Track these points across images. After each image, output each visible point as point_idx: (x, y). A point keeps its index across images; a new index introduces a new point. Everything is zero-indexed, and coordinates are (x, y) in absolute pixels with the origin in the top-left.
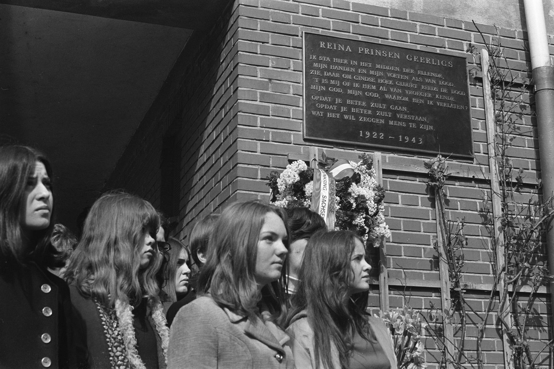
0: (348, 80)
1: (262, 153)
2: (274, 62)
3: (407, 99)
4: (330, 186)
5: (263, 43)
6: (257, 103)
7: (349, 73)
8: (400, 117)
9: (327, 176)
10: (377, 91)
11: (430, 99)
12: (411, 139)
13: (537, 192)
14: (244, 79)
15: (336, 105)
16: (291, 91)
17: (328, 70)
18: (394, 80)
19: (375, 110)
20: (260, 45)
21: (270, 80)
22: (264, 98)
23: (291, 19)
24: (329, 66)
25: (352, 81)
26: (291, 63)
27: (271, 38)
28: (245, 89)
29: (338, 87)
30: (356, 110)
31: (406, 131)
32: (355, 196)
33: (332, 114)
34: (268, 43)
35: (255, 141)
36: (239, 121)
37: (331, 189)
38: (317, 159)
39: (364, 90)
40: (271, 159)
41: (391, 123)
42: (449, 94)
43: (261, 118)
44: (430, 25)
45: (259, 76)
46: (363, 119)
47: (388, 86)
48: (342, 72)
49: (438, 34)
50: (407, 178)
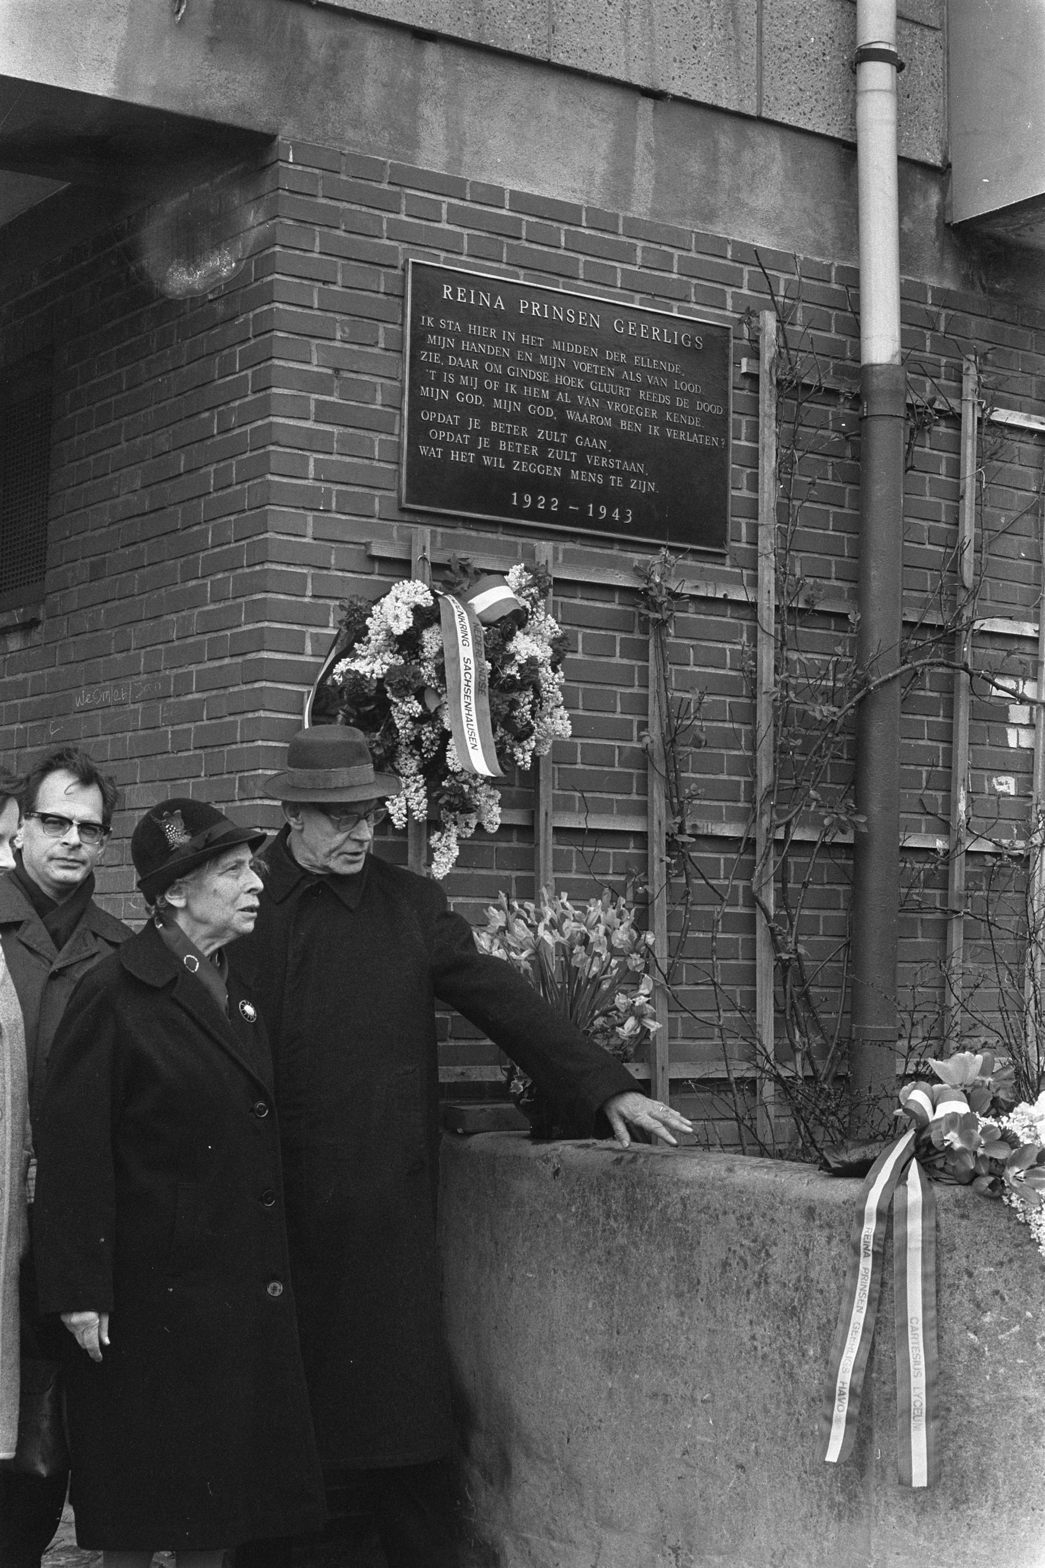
0: (494, 376)
1: (315, 539)
2: (347, 330)
3: (609, 422)
4: (474, 637)
5: (325, 282)
6: (309, 424)
7: (494, 359)
8: (593, 461)
9: (465, 615)
10: (552, 403)
11: (654, 422)
12: (610, 511)
13: (790, 1113)
14: (284, 367)
15: (468, 432)
16: (379, 398)
17: (458, 353)
18: (587, 377)
19: (544, 446)
20: (320, 288)
21: (337, 370)
22: (325, 412)
23: (385, 227)
24: (458, 343)
25: (504, 378)
26: (381, 332)
27: (341, 273)
28: (286, 392)
29: (474, 392)
30: (507, 446)
31: (603, 495)
32: (522, 662)
33: (460, 455)
34: (334, 283)
35: (301, 511)
36: (273, 466)
37: (476, 643)
38: (428, 558)
39: (525, 401)
40: (333, 552)
41: (575, 475)
42: (691, 412)
43: (316, 460)
44: (664, 248)
45: (315, 362)
46: (520, 466)
47: (574, 392)
48: (482, 358)
49: (678, 269)
50: (596, 595)
